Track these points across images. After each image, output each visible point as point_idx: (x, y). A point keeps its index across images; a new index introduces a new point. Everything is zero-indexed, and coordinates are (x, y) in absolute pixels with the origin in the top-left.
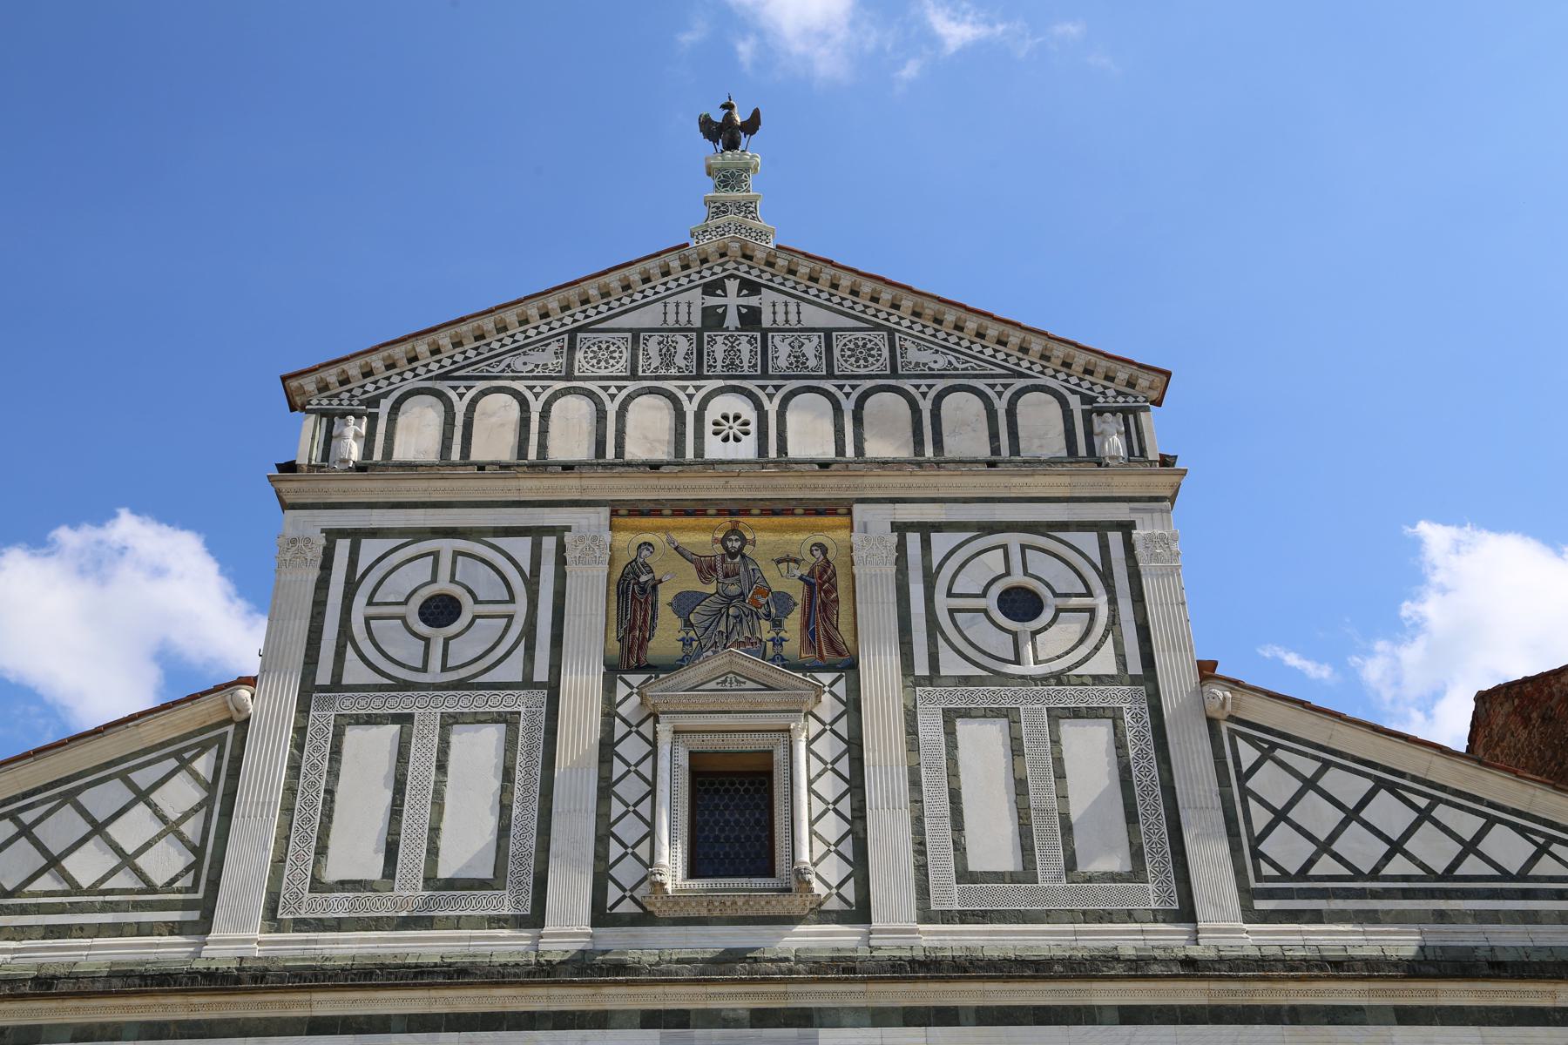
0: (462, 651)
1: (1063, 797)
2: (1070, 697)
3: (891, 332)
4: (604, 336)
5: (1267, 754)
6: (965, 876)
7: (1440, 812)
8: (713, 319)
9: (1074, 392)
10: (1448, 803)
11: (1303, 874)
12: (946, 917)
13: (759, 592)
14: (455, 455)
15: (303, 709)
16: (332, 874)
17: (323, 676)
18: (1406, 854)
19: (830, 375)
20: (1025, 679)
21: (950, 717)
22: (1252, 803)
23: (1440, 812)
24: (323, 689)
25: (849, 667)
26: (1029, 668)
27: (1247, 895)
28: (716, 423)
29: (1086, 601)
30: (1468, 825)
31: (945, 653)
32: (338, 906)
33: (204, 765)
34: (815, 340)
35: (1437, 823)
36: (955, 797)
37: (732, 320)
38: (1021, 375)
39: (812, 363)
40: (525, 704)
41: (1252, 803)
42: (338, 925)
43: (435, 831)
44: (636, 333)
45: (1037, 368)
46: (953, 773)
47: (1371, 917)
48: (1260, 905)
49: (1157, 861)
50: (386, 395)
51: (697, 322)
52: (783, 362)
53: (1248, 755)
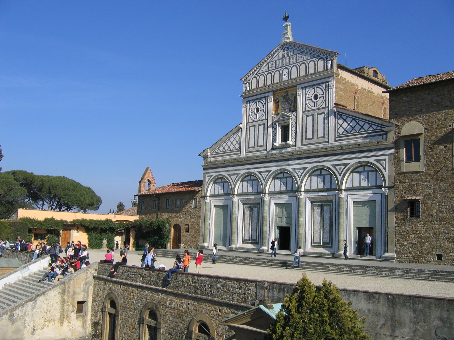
0: (260, 115)
1: (317, 127)
2: (320, 111)
3: (304, 52)
4: (272, 63)
5: (341, 117)
6: (306, 139)
7: (360, 123)
8: (284, 55)
9: (325, 58)
10: (361, 121)
11: (342, 134)
12: (304, 145)
13: (289, 100)
14: (258, 87)
15: (246, 126)
16: (250, 146)
17: (248, 122)
18: (355, 130)
19: (297, 63)
20: (315, 110)
21: (307, 116)
22: (338, 124)
23: (360, 123)
24: (248, 123)
25: (296, 111)
26: (316, 107)
27: (336, 137)
28: (284, 74)
29: (323, 95)
30: (361, 123)
31: (307, 107)
32: (251, 150)
33: (239, 134)
34: (295, 56)
35: (359, 124)
36: (306, 128)
37: (286, 56)
38: (319, 56)
39: (295, 61)
40: (265, 122)
41: (338, 124)
42: (251, 152)
43: (258, 140)
44: (275, 61)
45: (321, 54)
46: (306, 125)
47: (348, 139)
48: (337, 139)
49: (326, 134)
50: (251, 79)
51: (282, 57)
52: (291, 62)
53: (339, 116)
